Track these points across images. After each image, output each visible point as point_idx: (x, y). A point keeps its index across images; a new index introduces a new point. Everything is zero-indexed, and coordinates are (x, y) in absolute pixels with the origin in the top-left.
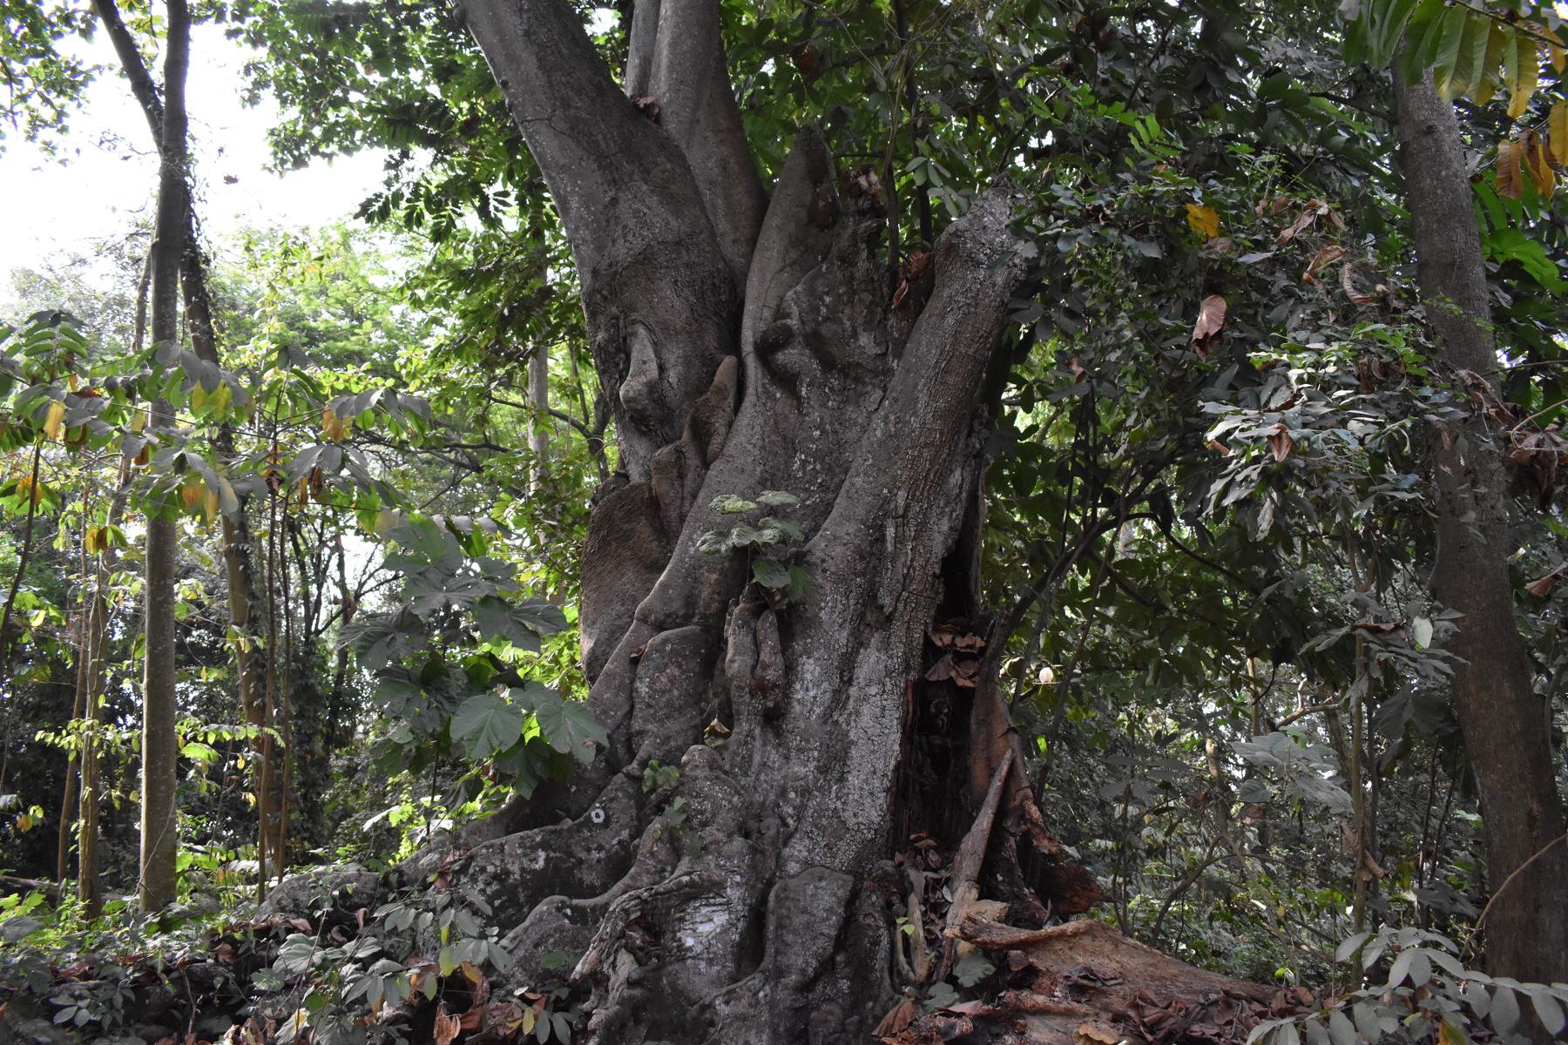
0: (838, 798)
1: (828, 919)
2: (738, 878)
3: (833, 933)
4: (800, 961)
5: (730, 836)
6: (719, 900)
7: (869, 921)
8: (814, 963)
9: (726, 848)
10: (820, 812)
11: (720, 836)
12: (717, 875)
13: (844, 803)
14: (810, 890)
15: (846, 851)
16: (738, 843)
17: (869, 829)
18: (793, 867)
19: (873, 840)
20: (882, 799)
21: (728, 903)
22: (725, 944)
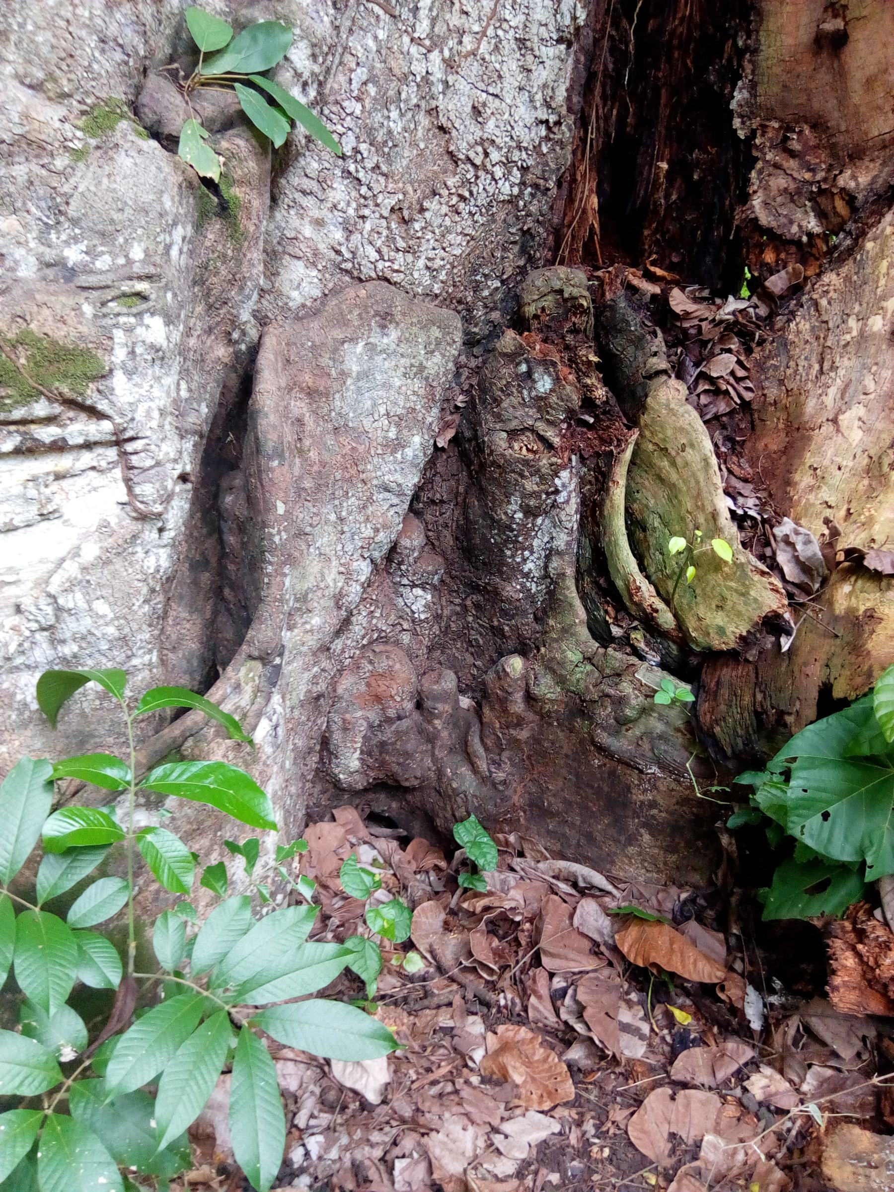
0: (435, 42)
1: (398, 445)
2: (155, 330)
3: (411, 480)
4: (333, 580)
5: (98, 120)
6: (79, 429)
7: (519, 449)
8: (364, 569)
9: (84, 180)
10: (389, 84)
11: (49, 116)
12: (66, 319)
13: (450, 65)
14: (354, 357)
15: (444, 243)
16: (137, 173)
17: (507, 163)
18: (301, 282)
19: (512, 201)
20: (554, 70)
21: (119, 441)
22: (123, 600)
